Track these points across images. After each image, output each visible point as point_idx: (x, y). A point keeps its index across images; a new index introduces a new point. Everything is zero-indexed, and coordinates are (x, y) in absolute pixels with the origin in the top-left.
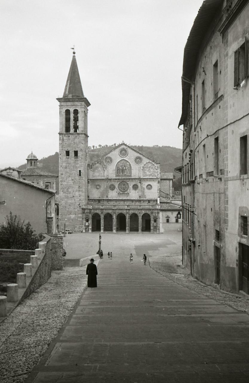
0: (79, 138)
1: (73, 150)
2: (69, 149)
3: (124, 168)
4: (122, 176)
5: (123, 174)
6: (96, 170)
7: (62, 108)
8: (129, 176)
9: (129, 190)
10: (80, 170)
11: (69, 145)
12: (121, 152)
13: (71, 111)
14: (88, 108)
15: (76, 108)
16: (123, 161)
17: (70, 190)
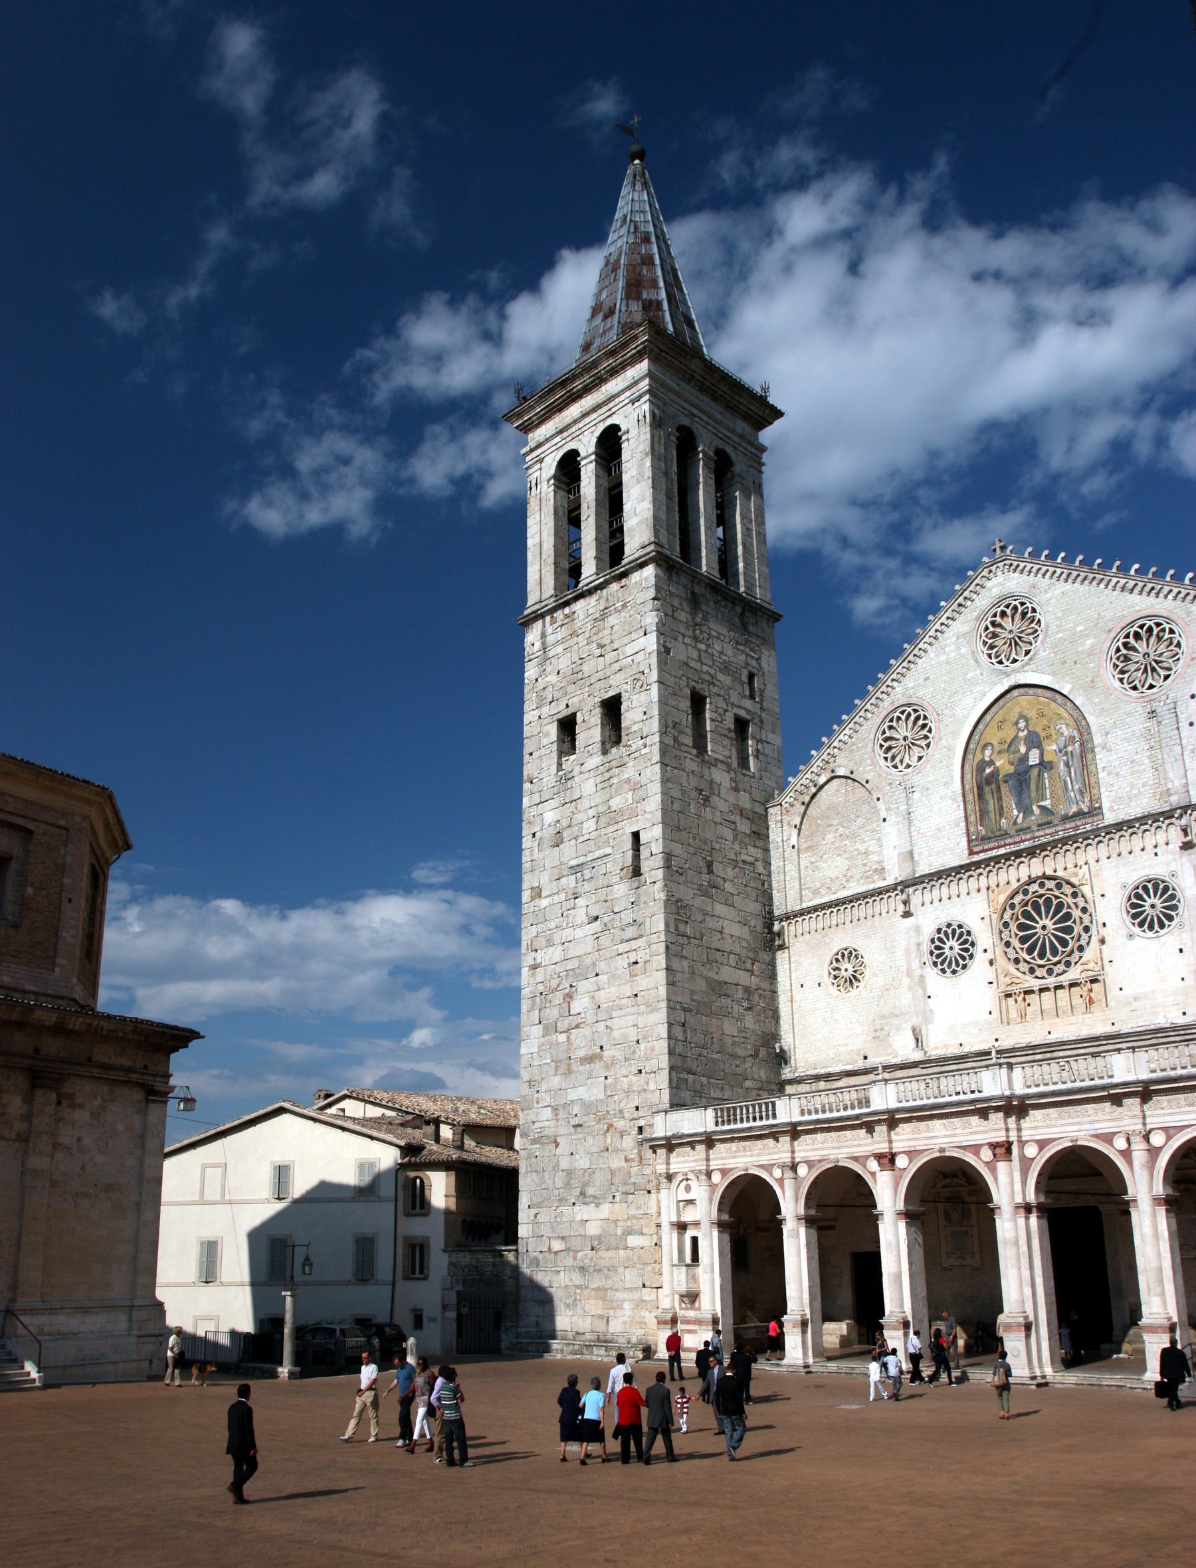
0: (624, 606)
1: (598, 700)
2: (574, 701)
3: (1034, 757)
4: (1019, 831)
5: (1027, 811)
6: (830, 837)
7: (541, 461)
8: (1080, 814)
9: (1094, 940)
10: (635, 829)
11: (576, 677)
12: (993, 630)
13: (583, 454)
14: (767, 436)
15: (609, 422)
16: (1023, 701)
17: (580, 1004)
